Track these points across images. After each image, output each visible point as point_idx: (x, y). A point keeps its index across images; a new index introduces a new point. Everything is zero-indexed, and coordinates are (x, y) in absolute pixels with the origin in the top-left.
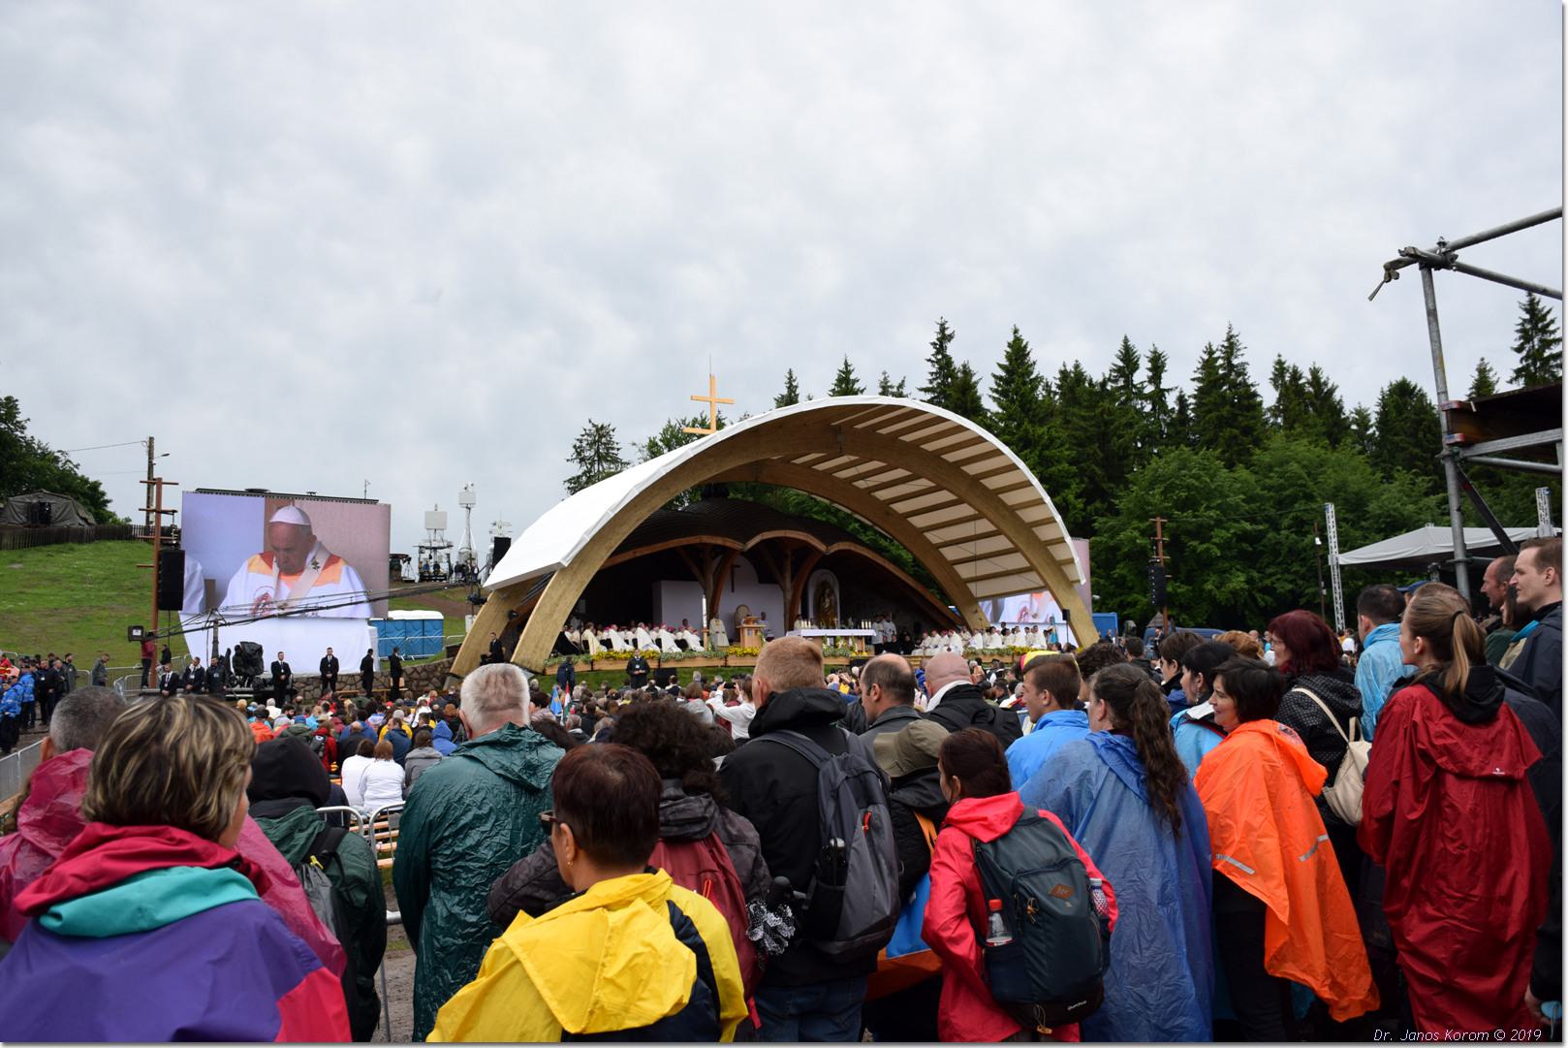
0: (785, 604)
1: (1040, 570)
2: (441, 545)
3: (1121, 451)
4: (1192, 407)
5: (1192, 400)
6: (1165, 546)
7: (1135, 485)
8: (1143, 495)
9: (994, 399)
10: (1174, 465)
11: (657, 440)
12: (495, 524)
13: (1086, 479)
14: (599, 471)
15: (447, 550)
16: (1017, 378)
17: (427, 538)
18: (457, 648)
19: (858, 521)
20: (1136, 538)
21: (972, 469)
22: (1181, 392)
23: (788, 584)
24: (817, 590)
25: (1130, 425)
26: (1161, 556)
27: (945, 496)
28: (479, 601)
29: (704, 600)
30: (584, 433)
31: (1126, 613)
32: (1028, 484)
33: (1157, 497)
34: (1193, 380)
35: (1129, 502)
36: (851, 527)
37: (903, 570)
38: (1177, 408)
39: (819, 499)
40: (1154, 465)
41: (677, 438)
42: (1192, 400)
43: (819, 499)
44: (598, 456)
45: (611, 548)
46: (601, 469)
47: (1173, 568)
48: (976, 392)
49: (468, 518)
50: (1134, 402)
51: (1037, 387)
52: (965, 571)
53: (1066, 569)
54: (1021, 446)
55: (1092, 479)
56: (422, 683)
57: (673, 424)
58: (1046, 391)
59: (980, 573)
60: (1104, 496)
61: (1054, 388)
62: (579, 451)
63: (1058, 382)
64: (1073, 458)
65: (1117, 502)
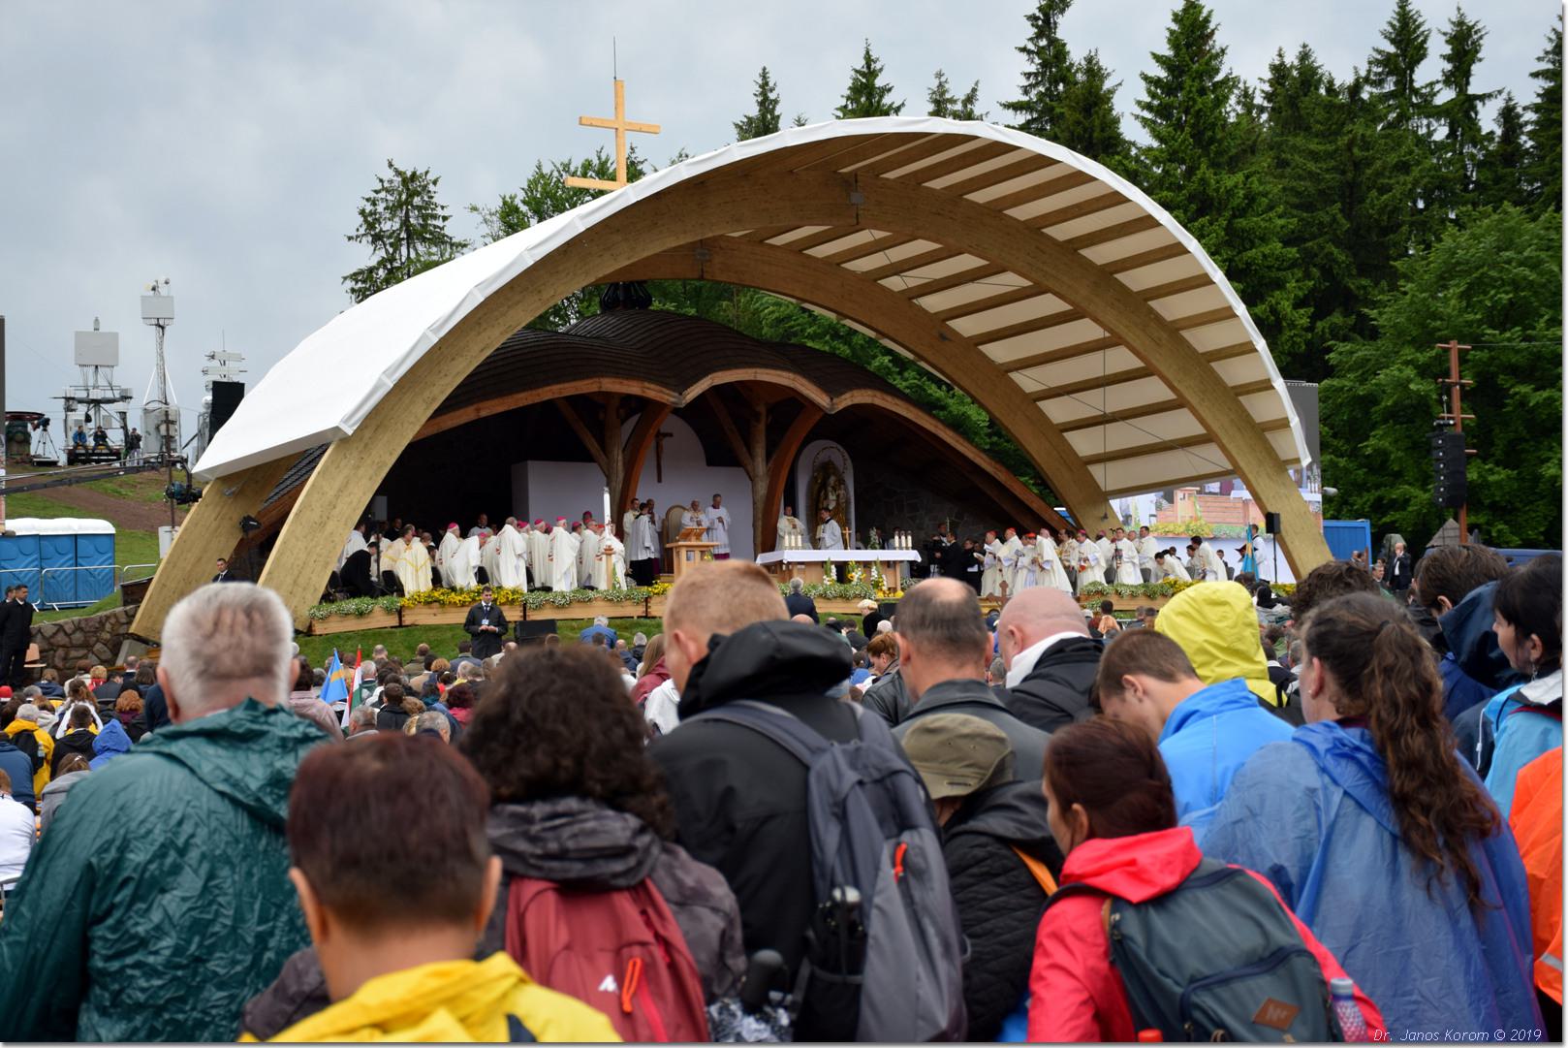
0: (754, 503)
1: (1224, 441)
2: (109, 395)
3: (1385, 218)
4: (1529, 128)
5: (1530, 116)
6: (1466, 395)
7: (1408, 279)
8: (1425, 299)
9: (1145, 122)
10: (1490, 241)
11: (517, 201)
12: (213, 357)
13: (1315, 272)
14: (408, 257)
15: (120, 406)
16: (1189, 82)
17: (81, 383)
18: (143, 586)
19: (889, 352)
20: (1409, 381)
21: (1101, 254)
22: (1510, 99)
23: (761, 466)
24: (814, 479)
25: (1404, 167)
26: (1457, 414)
27: (1048, 304)
28: (187, 495)
29: (607, 497)
30: (379, 186)
31: (1386, 519)
32: (1205, 281)
33: (1453, 302)
34: (1535, 75)
35: (1398, 312)
36: (876, 363)
37: (970, 440)
38: (1499, 132)
39: (817, 311)
40: (1448, 242)
41: (553, 197)
42: (1530, 116)
43: (817, 311)
44: (408, 231)
45: (434, 399)
46: (413, 255)
47: (1481, 437)
48: (1111, 109)
49: (161, 344)
50: (1414, 123)
51: (1226, 98)
52: (1084, 443)
53: (1275, 439)
54: (1194, 209)
55: (1327, 272)
56: (73, 653)
57: (546, 170)
58: (1244, 105)
59: (1112, 447)
60: (1348, 301)
61: (1259, 100)
62: (370, 220)
63: (1267, 88)
64: (1293, 232)
65: (1374, 313)
